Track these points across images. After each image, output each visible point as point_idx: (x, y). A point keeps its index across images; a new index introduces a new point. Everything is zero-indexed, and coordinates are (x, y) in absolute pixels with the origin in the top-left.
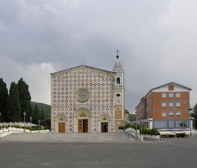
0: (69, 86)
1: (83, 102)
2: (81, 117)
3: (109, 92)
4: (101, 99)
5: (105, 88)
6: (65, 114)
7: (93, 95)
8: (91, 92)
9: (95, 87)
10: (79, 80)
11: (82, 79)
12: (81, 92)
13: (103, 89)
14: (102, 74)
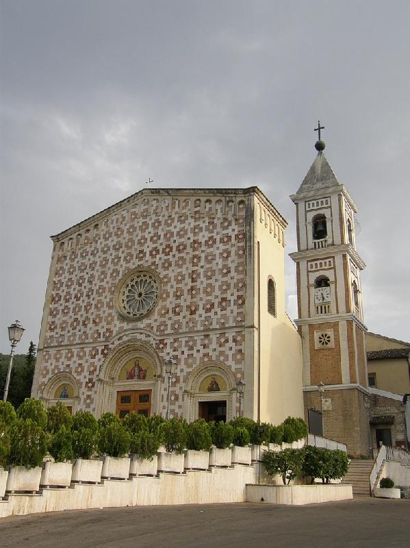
2: (131, 382)
3: (232, 266)
5: (217, 252)
8: (165, 277)
14: (208, 205)
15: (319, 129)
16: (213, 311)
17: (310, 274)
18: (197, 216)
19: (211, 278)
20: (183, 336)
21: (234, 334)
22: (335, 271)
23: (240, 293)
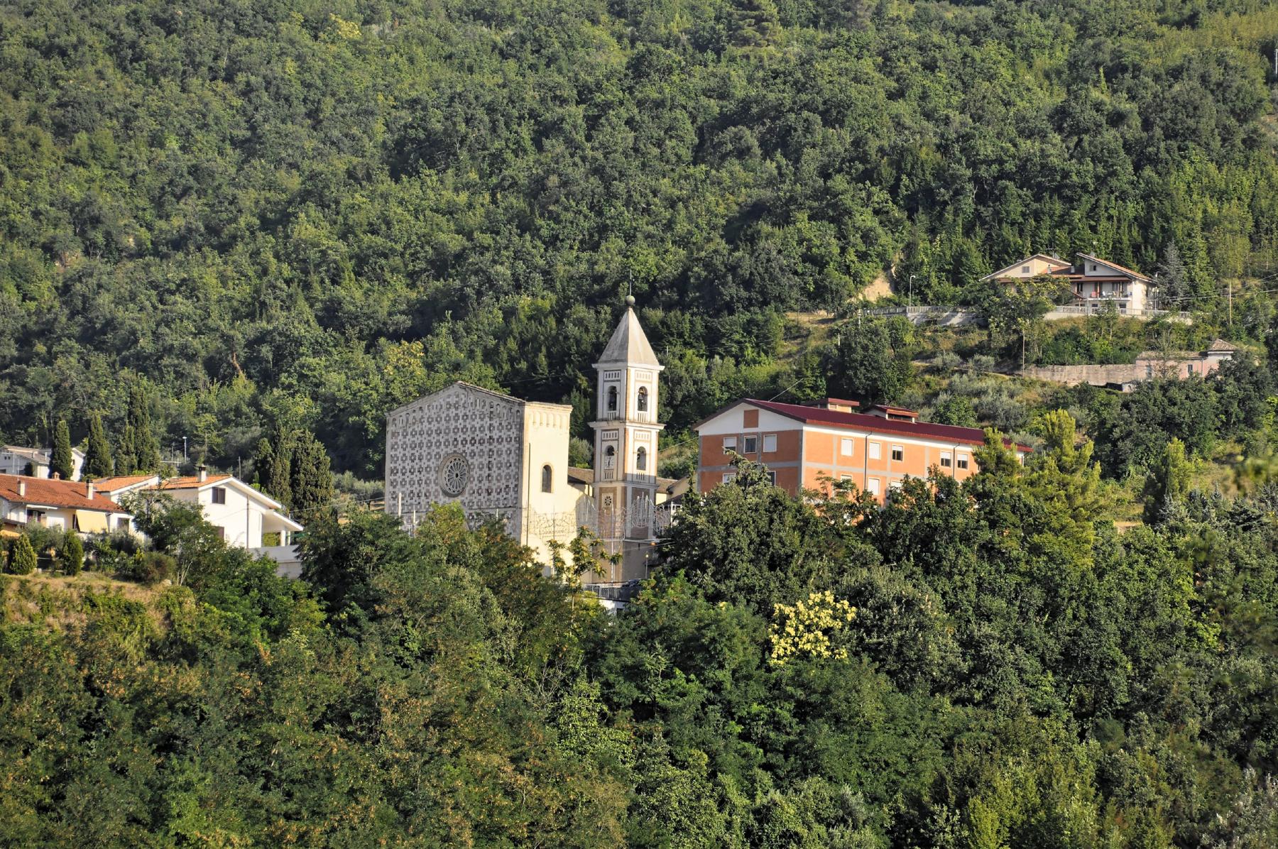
7: (476, 473)
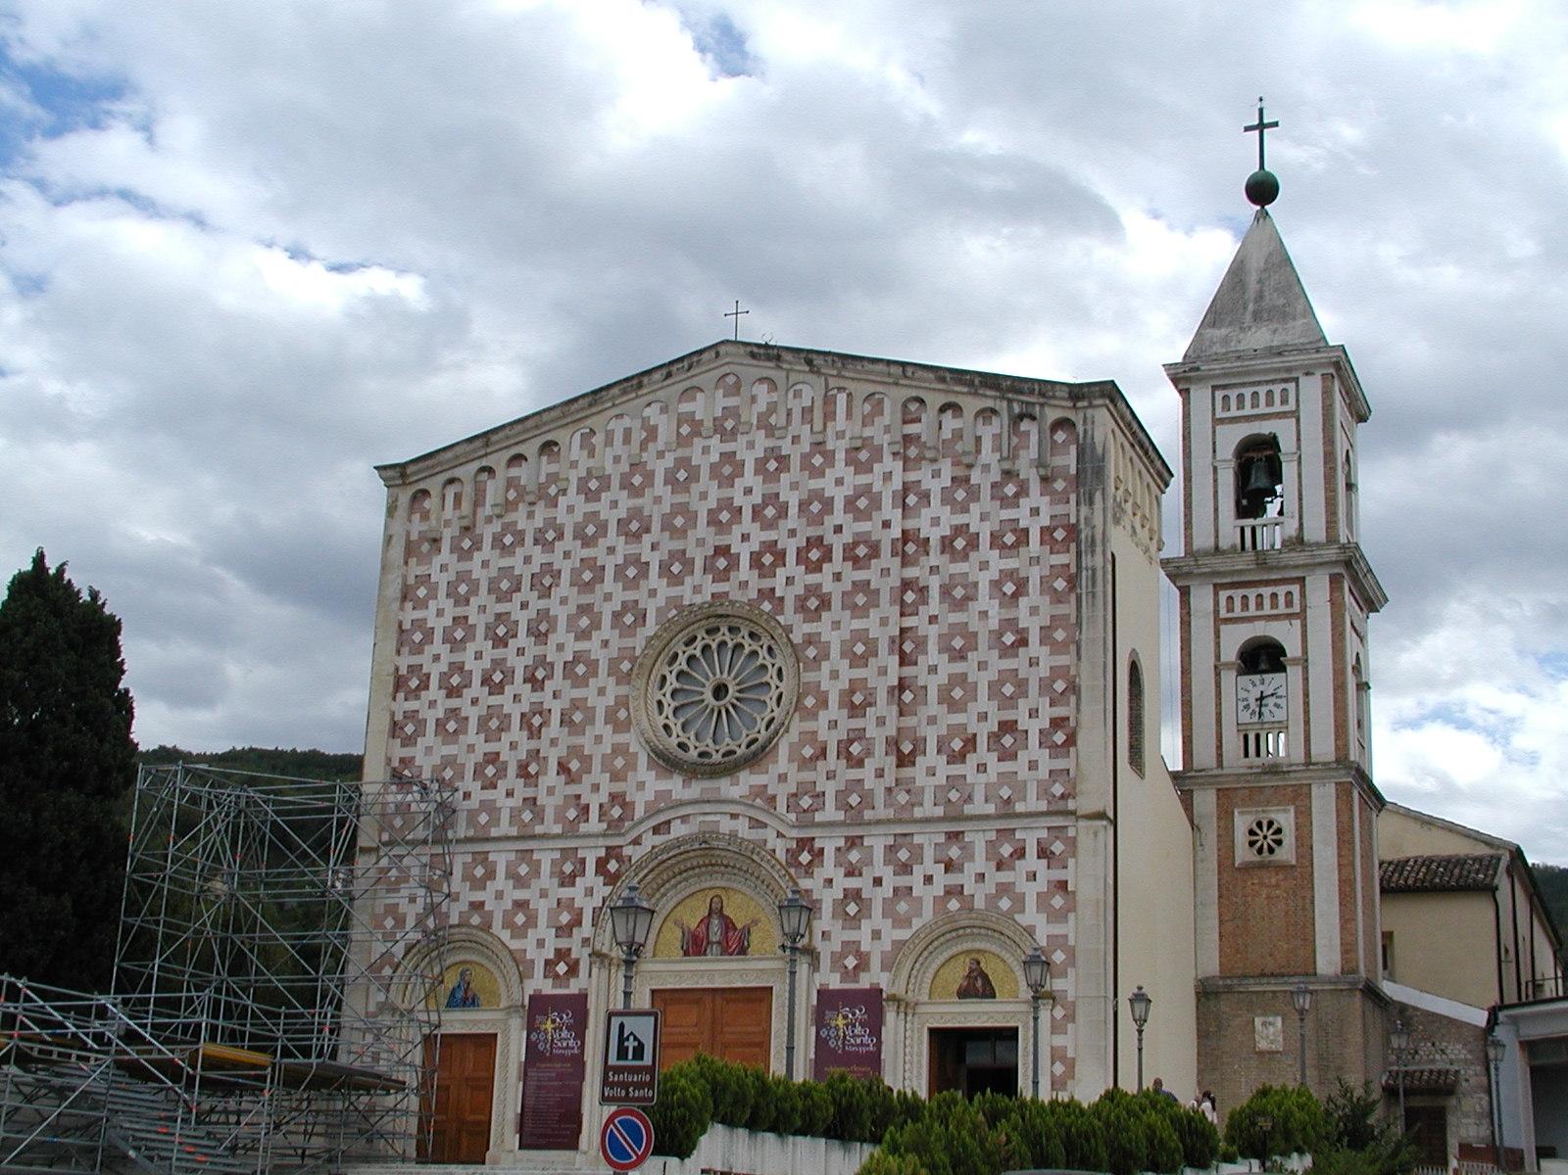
0: (564, 588)
1: (716, 772)
2: (696, 965)
3: (1033, 625)
4: (932, 720)
5: (984, 579)
6: (497, 927)
7: (833, 677)
8: (810, 640)
9: (861, 575)
10: (681, 509)
11: (715, 493)
12: (696, 650)
13: (960, 596)
15: (1261, 127)
16: (972, 759)
17: (1223, 627)
18: (913, 452)
19: (963, 658)
20: (875, 830)
21: (1044, 834)
22: (1304, 626)
23: (1060, 711)
